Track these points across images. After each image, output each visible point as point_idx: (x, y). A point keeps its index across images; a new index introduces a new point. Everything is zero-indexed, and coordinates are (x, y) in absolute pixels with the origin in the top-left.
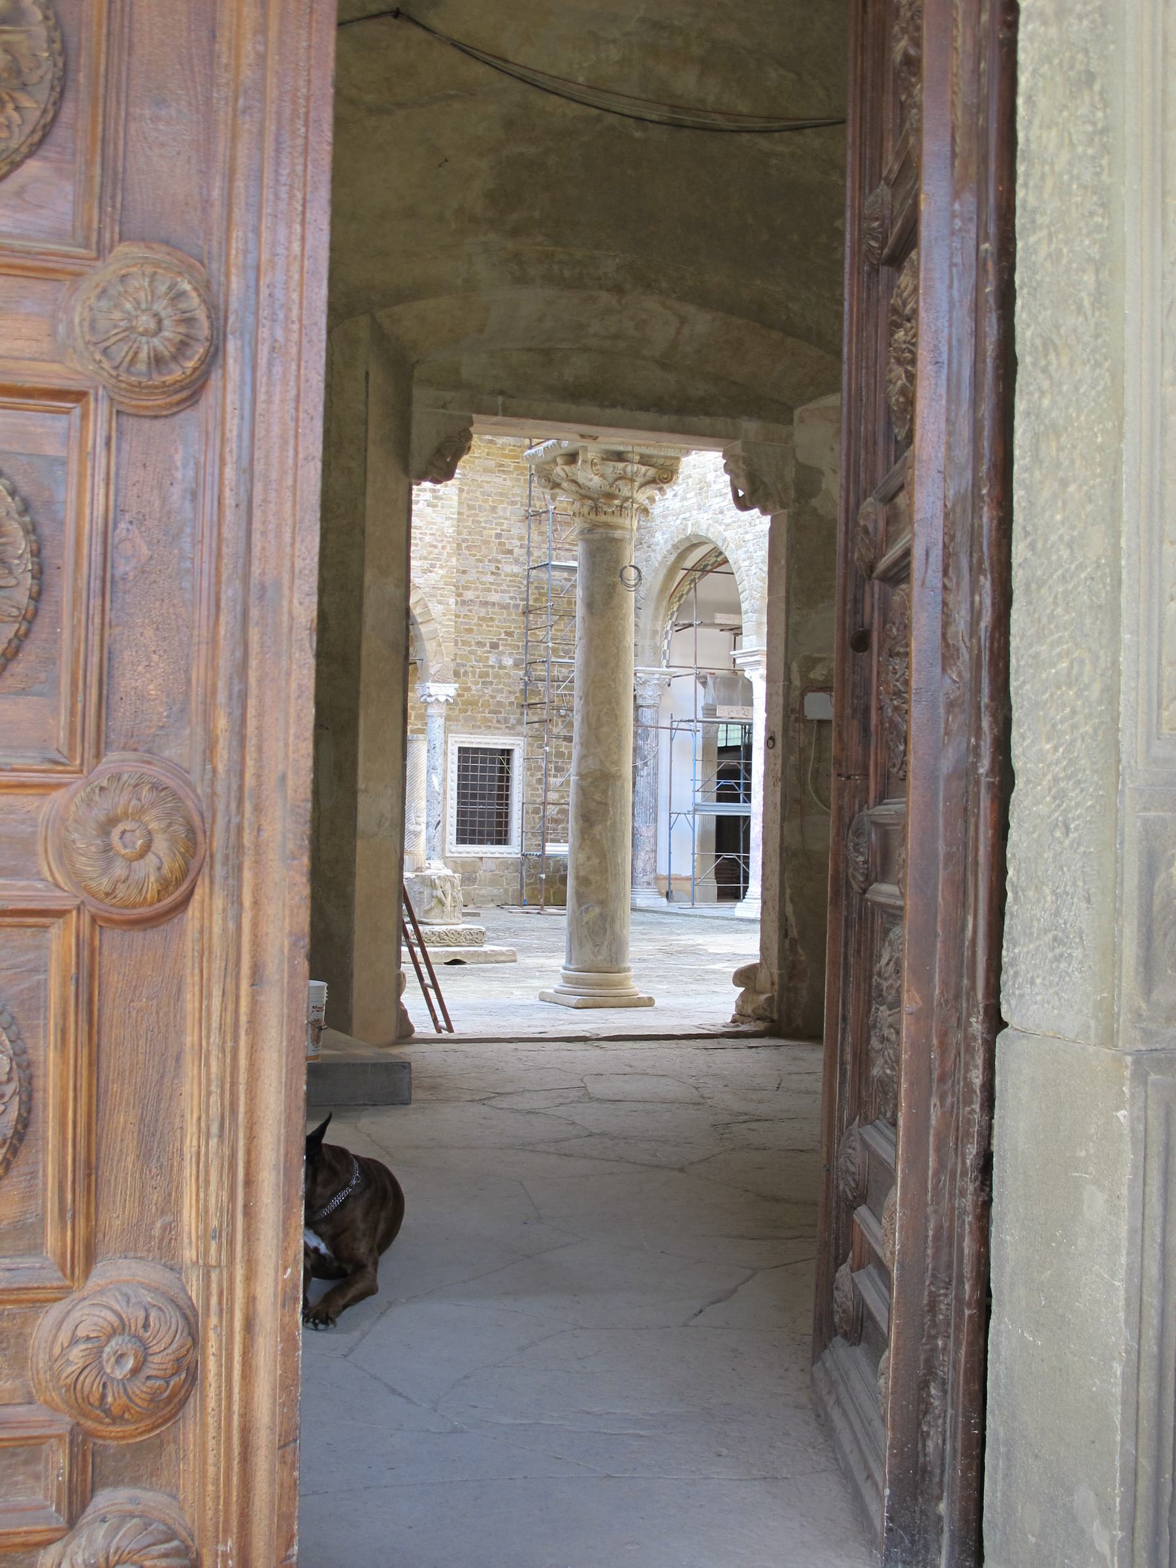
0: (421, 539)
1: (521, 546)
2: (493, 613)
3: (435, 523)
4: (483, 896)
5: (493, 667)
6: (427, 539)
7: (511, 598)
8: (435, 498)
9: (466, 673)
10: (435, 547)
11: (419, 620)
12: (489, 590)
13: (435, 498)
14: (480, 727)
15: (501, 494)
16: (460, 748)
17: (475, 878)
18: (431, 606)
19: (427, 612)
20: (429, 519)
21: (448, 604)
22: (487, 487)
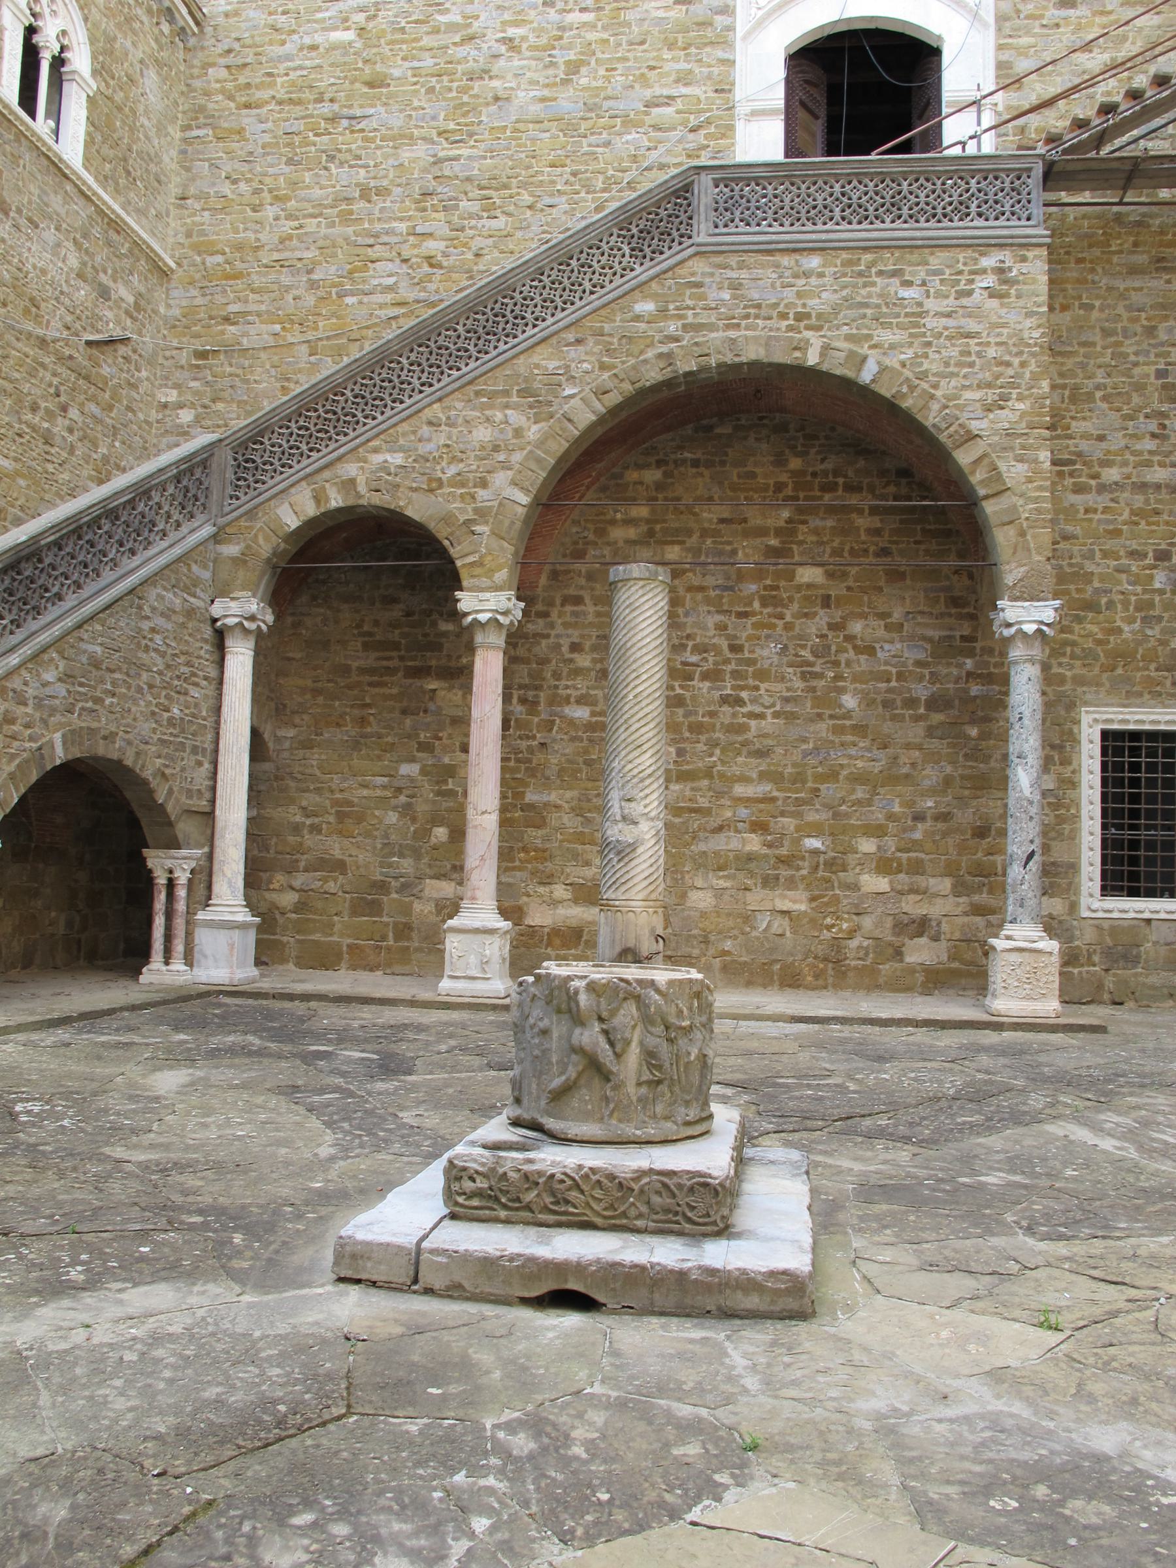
0: (979, 354)
2: (1158, 501)
3: (1004, 325)
4: (1153, 987)
5: (1161, 592)
6: (992, 352)
9: (1111, 604)
10: (1008, 364)
11: (982, 492)
12: (1148, 464)
13: (1005, 282)
14: (1140, 695)
15: (1163, 307)
16: (1105, 734)
17: (1138, 956)
18: (1002, 466)
20: (994, 319)
21: (1036, 461)
22: (1135, 297)
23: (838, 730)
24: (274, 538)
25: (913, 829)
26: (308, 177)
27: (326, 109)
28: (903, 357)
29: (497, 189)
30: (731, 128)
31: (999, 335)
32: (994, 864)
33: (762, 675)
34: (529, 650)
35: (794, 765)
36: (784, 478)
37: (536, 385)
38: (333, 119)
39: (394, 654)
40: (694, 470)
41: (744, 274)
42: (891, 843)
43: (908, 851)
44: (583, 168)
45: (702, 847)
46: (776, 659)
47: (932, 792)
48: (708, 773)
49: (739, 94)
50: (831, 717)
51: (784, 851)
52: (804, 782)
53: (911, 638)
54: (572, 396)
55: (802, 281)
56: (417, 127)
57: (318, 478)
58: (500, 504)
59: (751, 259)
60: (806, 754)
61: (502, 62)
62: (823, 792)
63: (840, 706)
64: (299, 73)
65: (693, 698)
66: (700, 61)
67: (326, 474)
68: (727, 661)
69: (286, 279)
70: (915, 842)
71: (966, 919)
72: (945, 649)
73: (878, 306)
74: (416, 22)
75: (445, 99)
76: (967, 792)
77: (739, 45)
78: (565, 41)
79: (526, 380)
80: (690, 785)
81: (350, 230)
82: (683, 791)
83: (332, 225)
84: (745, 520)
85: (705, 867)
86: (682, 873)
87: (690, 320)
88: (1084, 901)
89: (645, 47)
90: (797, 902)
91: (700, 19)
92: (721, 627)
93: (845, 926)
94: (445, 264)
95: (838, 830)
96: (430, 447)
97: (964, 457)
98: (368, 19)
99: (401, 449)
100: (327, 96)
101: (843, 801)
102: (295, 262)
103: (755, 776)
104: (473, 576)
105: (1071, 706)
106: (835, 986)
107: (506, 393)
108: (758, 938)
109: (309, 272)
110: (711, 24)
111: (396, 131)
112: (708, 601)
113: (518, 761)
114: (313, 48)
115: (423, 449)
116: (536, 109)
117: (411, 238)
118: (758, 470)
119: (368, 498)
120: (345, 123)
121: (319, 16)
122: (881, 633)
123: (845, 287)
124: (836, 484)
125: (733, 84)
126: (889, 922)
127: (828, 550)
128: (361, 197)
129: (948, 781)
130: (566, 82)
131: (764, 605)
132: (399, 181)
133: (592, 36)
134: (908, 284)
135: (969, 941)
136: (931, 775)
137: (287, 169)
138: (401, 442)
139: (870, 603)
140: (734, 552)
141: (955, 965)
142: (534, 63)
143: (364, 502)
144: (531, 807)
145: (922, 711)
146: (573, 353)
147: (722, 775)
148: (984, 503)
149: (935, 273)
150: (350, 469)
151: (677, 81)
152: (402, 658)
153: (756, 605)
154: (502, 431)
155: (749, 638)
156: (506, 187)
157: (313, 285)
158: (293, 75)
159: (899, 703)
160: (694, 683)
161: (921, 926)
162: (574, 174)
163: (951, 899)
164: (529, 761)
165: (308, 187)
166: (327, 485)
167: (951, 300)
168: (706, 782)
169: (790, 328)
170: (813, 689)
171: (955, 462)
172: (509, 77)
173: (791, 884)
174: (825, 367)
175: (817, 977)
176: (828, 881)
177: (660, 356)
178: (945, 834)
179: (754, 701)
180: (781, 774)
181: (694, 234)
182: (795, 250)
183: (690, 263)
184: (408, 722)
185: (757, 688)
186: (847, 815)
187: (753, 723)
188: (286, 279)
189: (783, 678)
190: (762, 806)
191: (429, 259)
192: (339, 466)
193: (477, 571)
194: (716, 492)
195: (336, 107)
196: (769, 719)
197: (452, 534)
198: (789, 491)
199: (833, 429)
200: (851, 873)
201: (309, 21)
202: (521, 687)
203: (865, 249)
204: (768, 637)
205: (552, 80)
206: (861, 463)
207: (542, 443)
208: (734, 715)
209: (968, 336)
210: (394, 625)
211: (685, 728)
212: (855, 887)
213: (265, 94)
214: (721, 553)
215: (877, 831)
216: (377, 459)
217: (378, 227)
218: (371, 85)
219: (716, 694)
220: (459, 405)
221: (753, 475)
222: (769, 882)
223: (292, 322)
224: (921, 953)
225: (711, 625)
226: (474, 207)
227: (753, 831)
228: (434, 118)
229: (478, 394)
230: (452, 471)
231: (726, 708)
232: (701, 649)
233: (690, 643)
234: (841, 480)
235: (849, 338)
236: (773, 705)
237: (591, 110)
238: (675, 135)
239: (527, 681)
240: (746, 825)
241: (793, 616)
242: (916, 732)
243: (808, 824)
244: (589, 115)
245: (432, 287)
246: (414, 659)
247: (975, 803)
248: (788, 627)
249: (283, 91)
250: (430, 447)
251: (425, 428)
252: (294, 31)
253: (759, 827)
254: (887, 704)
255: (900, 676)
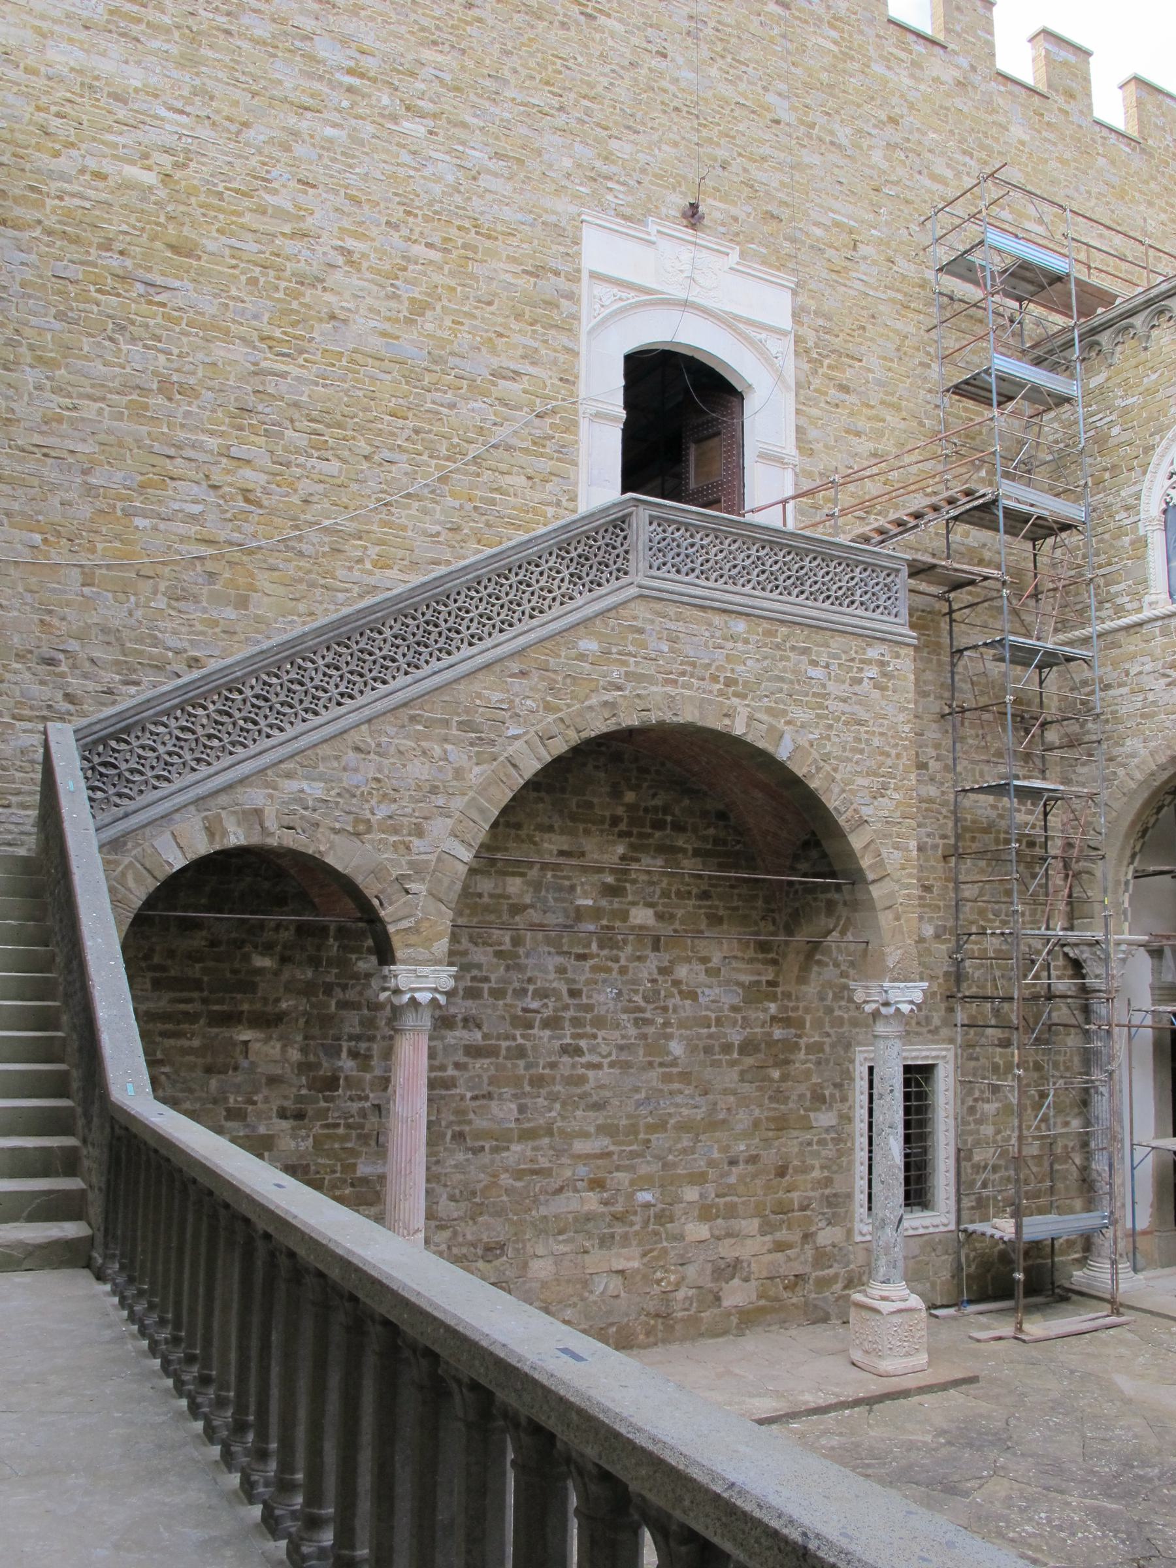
1: (938, 758)
3: (884, 717)
6: (876, 742)
7: (928, 835)
8: (885, 674)
10: (888, 755)
11: (871, 876)
18: (884, 851)
19: (881, 864)
21: (907, 849)
23: (667, 1078)
24: (150, 880)
25: (728, 1174)
26: (86, 344)
27: (114, 261)
28: (811, 736)
29: (328, 426)
30: (575, 424)
31: (881, 725)
32: (792, 1201)
33: (599, 1022)
34: (361, 994)
35: (629, 1117)
36: (620, 811)
37: (479, 719)
38: (123, 278)
39: (195, 995)
40: (535, 794)
41: (680, 626)
42: (711, 1189)
43: (723, 1195)
44: (427, 427)
45: (543, 1211)
46: (611, 1004)
47: (746, 1135)
48: (549, 1132)
49: (582, 390)
50: (661, 1065)
51: (619, 1208)
52: (636, 1133)
53: (728, 982)
54: (516, 737)
55: (730, 645)
56: (234, 321)
57: (212, 803)
58: (439, 859)
59: (688, 612)
60: (639, 1104)
61: (338, 275)
62: (654, 1144)
63: (668, 1053)
64: (77, 202)
65: (535, 1048)
66: (546, 342)
67: (223, 799)
68: (566, 1007)
69: (51, 473)
70: (730, 1186)
71: (770, 1257)
72: (755, 994)
73: (792, 682)
74: (237, 191)
75: (270, 298)
76: (771, 1134)
77: (583, 338)
78: (409, 274)
79: (467, 711)
80: (530, 1144)
81: (144, 429)
82: (524, 1151)
83: (119, 417)
84: (583, 854)
85: (546, 1233)
86: (523, 1241)
87: (632, 668)
88: (858, 1226)
89: (493, 308)
90: (629, 1259)
91: (547, 297)
92: (561, 970)
93: (672, 1278)
94: (265, 503)
95: (667, 1182)
96: (358, 778)
97: (857, 842)
98: (176, 165)
99: (321, 778)
100: (118, 246)
101: (670, 1150)
102: (65, 455)
103: (592, 1130)
104: (408, 946)
105: (848, 1046)
106: (665, 1341)
107: (446, 723)
108: (595, 1303)
109: (85, 472)
110: (558, 307)
111: (207, 319)
112: (548, 941)
113: (348, 1126)
114: (99, 176)
115: (349, 779)
116: (376, 343)
117: (224, 460)
118: (596, 800)
119: (279, 838)
120: (140, 288)
121: (110, 137)
122: (702, 977)
123: (766, 658)
124: (665, 822)
125: (577, 377)
126: (709, 1268)
127: (658, 892)
128: (160, 390)
129: (756, 1124)
130: (410, 322)
131: (601, 947)
132: (210, 383)
133: (437, 278)
134: (814, 663)
135: (771, 1278)
136: (743, 1120)
137: (58, 325)
138: (321, 768)
139: (693, 947)
140: (572, 888)
141: (762, 1302)
142: (376, 288)
143: (273, 842)
144: (365, 1181)
145: (735, 1056)
146: (517, 685)
147: (562, 1132)
148: (871, 888)
149: (836, 656)
150: (255, 796)
151: (524, 357)
152: (205, 1001)
153: (594, 946)
154: (440, 769)
155: (588, 982)
156: (340, 426)
157: (90, 490)
158: (68, 202)
159: (717, 1049)
160: (535, 1031)
161: (730, 1270)
162: (417, 432)
163: (759, 1239)
164: (362, 1127)
165: (86, 358)
166: (224, 814)
167: (846, 686)
168: (546, 1140)
169: (721, 693)
170: (644, 1037)
171: (849, 844)
172: (347, 295)
173: (626, 1239)
174: (749, 739)
175: (648, 1334)
176: (656, 1233)
177: (606, 703)
178: (755, 1176)
179: (592, 1050)
180: (617, 1126)
181: (632, 569)
182: (725, 611)
183: (632, 605)
184: (214, 1083)
185: (595, 1037)
186: (674, 1165)
187: (591, 1074)
188: (51, 473)
189: (618, 1025)
190: (600, 1162)
191: (246, 494)
192: (240, 789)
193: (413, 939)
194: (557, 823)
195: (129, 263)
196: (606, 1069)
197: (382, 891)
198: (623, 827)
199: (663, 764)
200: (676, 1224)
201: (94, 139)
202: (351, 1038)
203: (782, 622)
204: (604, 981)
205: (393, 314)
206: (686, 802)
207: (485, 789)
208: (574, 1066)
209: (859, 723)
210: (194, 957)
211: (526, 1082)
212: (680, 1237)
213: (30, 215)
214: (560, 889)
215: (699, 1179)
216: (292, 786)
217: (181, 435)
218: (172, 247)
219: (557, 1044)
220: (391, 730)
221: (590, 805)
222: (605, 1241)
223: (59, 535)
224: (737, 1295)
225: (551, 968)
226: (302, 440)
227: (592, 1189)
228: (256, 317)
229: (413, 719)
230: (382, 812)
231: (566, 1059)
232: (542, 994)
233: (531, 988)
234: (669, 818)
235: (770, 711)
236: (610, 1054)
237: (435, 362)
238: (524, 415)
239: (357, 1030)
240: (585, 1184)
241: (628, 959)
242: (731, 1077)
243: (640, 1177)
244: (434, 367)
245: (249, 528)
246: (221, 1001)
247: (776, 1143)
248: (623, 971)
249: (54, 218)
250: (358, 778)
251: (351, 754)
252: (73, 145)
253: (597, 1184)
254: (708, 1050)
255: (719, 1022)
